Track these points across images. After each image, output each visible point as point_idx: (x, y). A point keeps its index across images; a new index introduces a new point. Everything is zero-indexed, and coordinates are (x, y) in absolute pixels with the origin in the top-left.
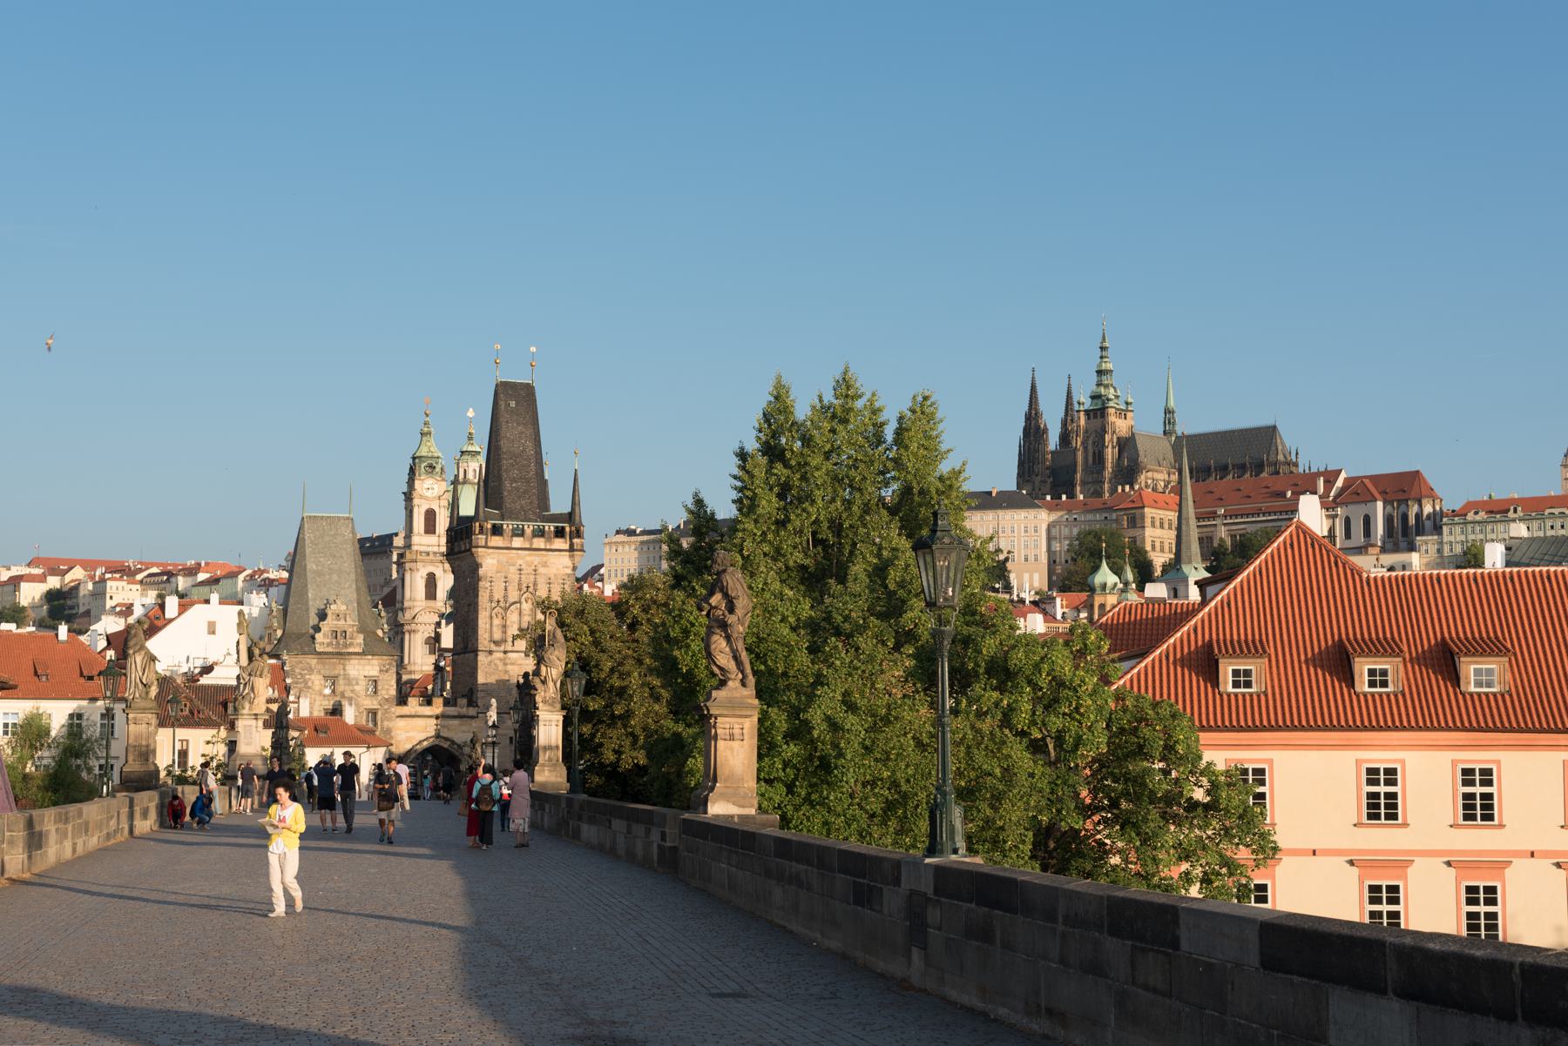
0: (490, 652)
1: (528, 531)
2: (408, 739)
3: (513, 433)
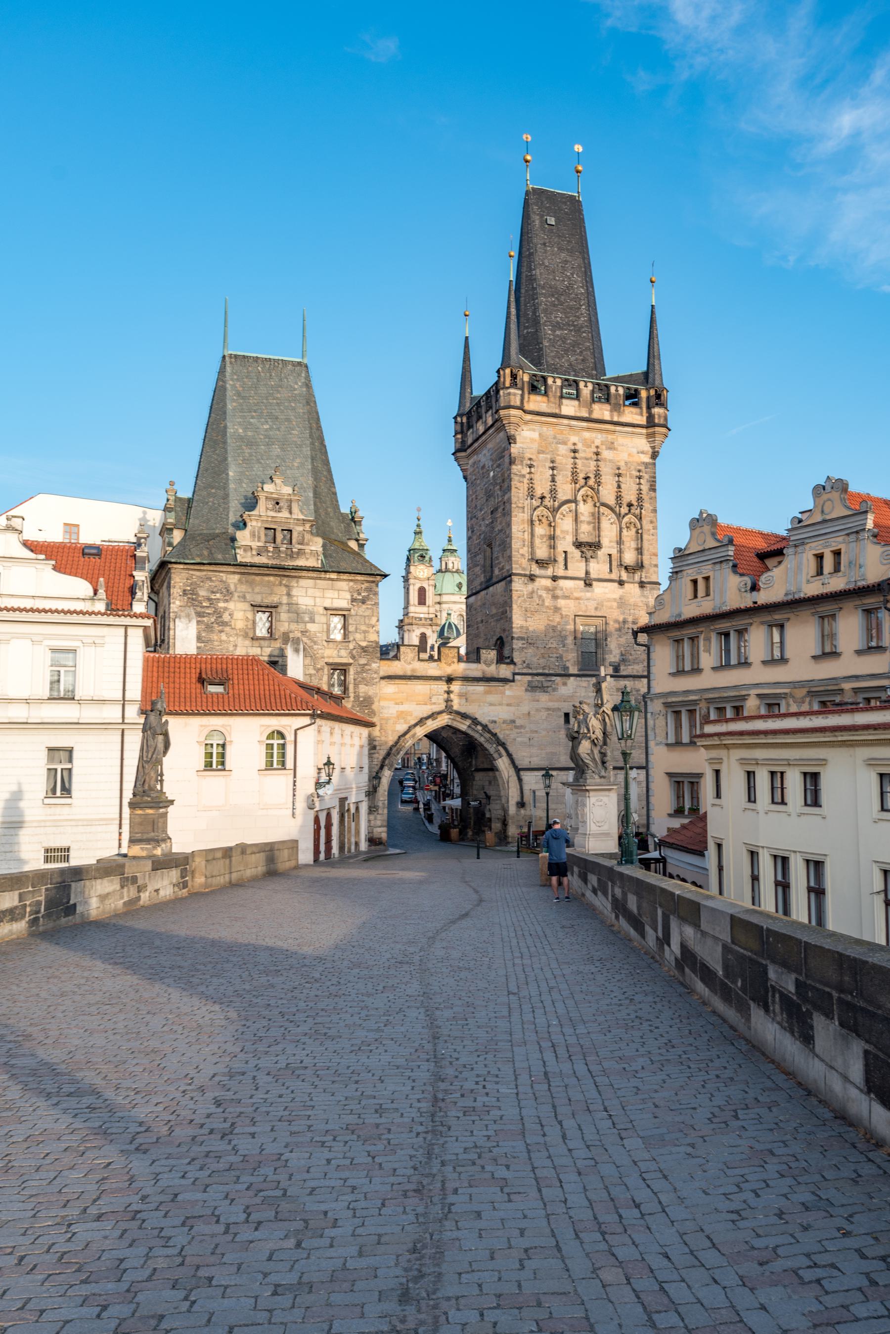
0: (532, 578)
1: (586, 390)
2: (401, 715)
3: (550, 259)
